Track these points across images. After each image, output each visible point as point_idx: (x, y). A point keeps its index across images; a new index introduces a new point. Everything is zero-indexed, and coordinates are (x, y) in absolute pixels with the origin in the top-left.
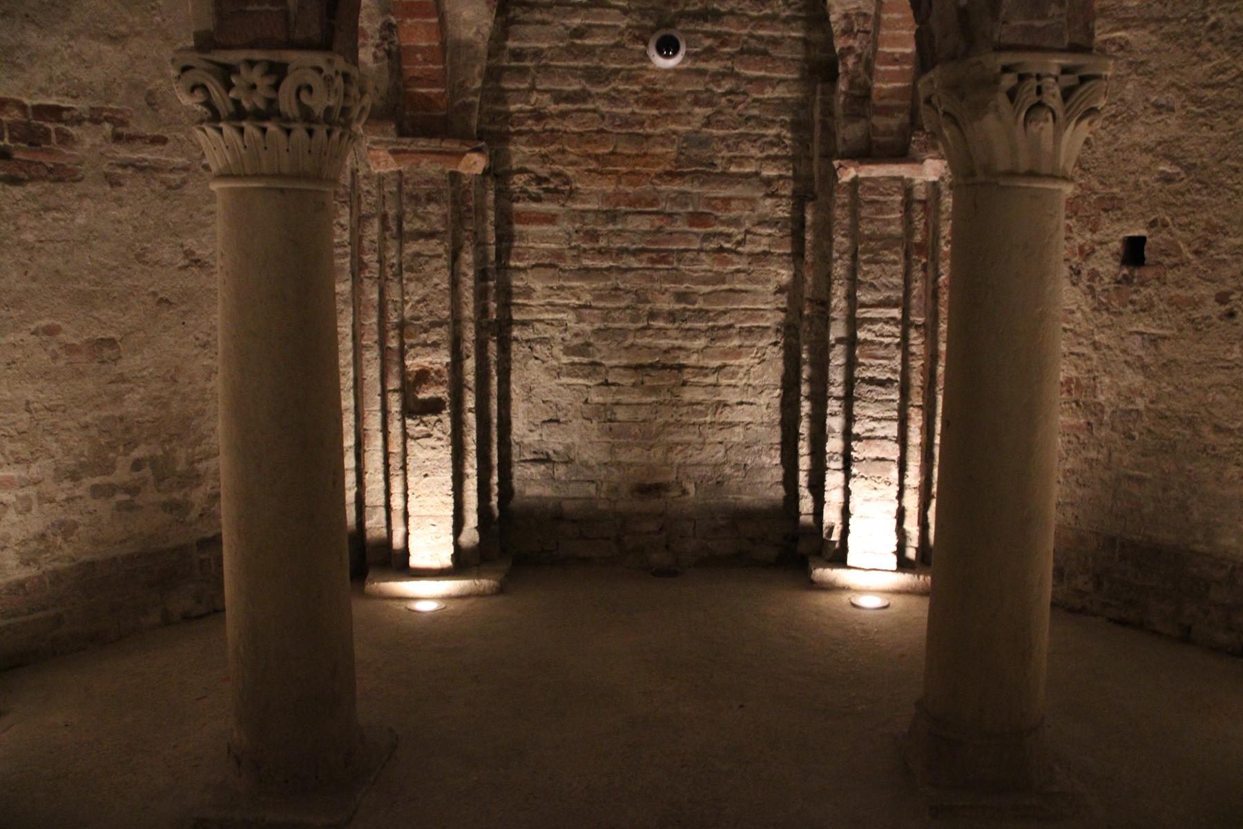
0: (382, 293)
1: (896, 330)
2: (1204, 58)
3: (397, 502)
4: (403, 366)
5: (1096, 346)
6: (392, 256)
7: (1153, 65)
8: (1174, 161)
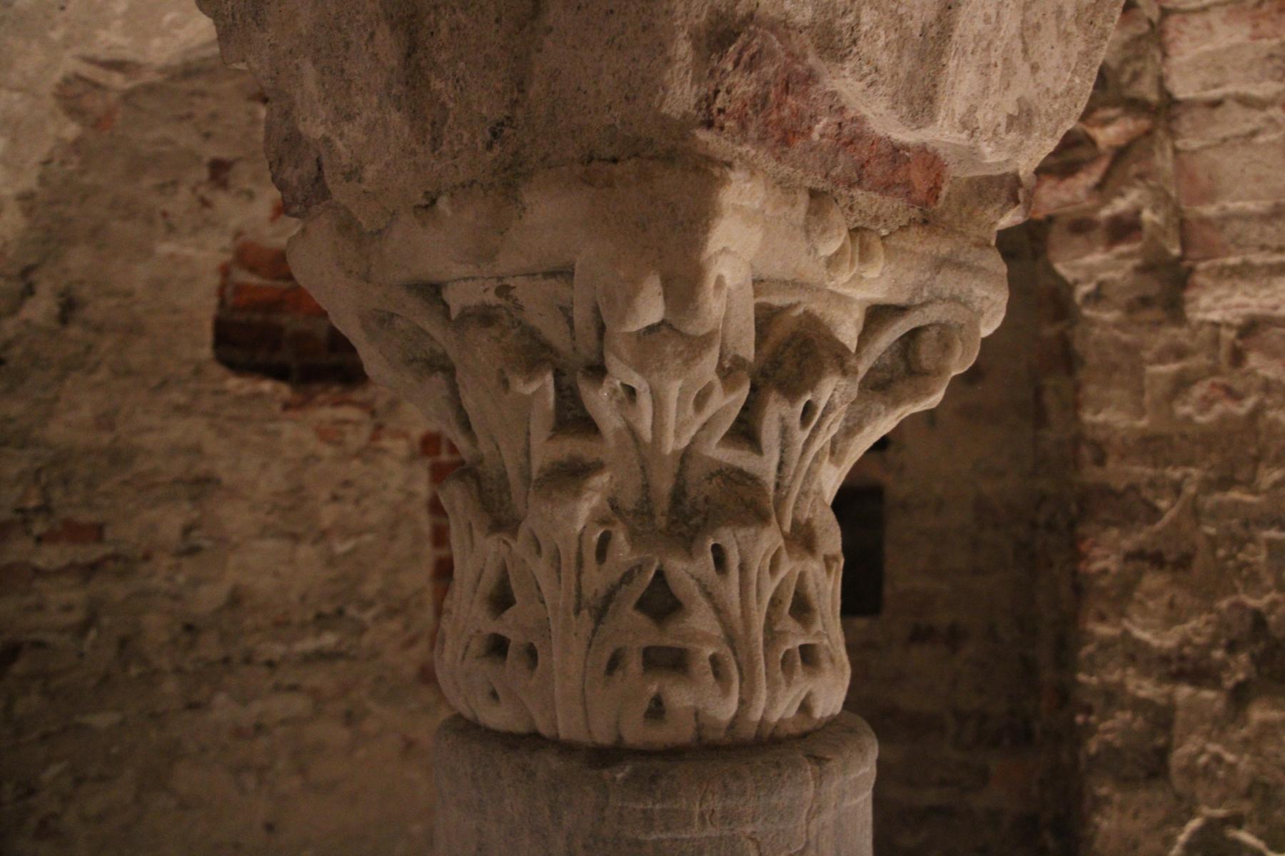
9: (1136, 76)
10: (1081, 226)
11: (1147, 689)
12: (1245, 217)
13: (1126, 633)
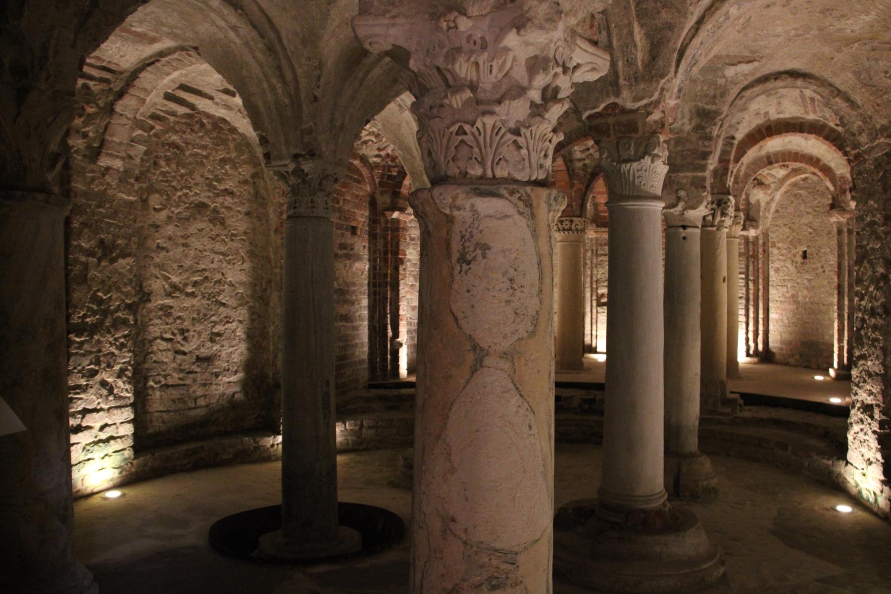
0: (591, 272)
1: (743, 281)
2: (816, 199)
3: (594, 333)
4: (597, 293)
5: (798, 283)
6: (594, 261)
8: (811, 227)
9: (100, 99)
10: (78, 132)
11: (83, 259)
12: (116, 143)
13: (80, 244)
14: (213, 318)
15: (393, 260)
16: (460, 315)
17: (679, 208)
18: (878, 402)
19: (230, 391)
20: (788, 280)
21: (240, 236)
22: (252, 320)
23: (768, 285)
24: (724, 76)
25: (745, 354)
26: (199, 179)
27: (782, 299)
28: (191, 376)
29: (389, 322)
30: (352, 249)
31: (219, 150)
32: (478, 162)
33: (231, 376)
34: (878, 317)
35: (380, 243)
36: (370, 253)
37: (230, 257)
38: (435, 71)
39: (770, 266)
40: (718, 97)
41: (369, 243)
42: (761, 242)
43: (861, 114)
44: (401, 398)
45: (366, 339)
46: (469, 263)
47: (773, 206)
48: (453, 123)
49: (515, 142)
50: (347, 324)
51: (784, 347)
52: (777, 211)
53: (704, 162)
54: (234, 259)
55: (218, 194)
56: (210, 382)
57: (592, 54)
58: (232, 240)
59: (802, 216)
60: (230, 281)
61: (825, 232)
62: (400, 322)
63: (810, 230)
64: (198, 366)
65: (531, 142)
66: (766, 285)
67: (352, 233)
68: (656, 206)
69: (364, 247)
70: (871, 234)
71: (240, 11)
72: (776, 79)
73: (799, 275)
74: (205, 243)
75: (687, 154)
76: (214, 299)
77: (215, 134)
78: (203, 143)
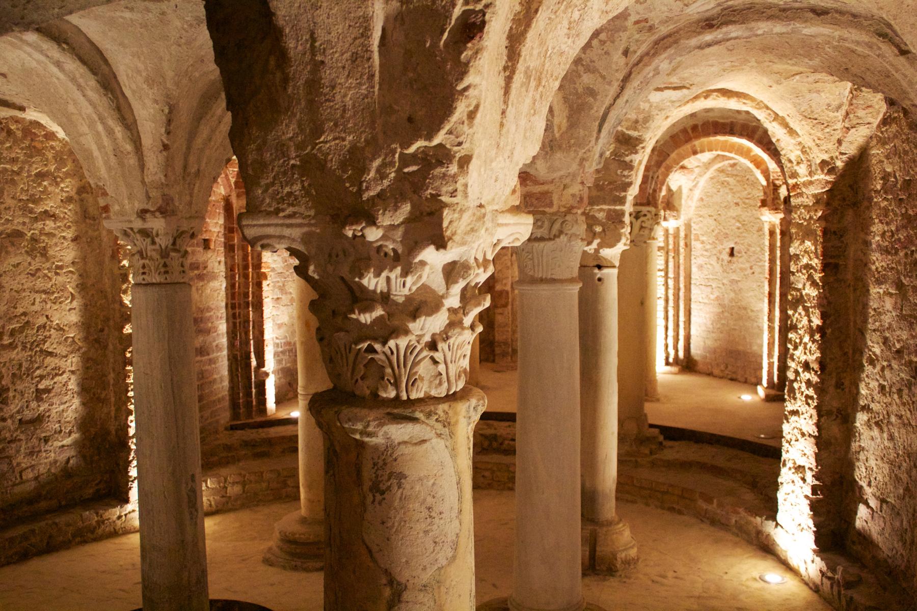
5: (723, 284)
7: (735, 190)
14: (38, 372)
15: (255, 275)
16: (375, 549)
17: (594, 245)
18: (811, 466)
19: (62, 457)
20: (713, 279)
21: (67, 267)
22: (87, 368)
23: (690, 283)
24: (648, 101)
25: (664, 362)
26: (9, 202)
27: (706, 301)
28: (13, 445)
29: (252, 350)
30: (205, 267)
31: (33, 162)
32: (391, 383)
33: (63, 438)
34: (813, 373)
35: (238, 257)
36: (226, 269)
37: (56, 295)
38: (338, 280)
39: (692, 262)
40: (640, 123)
41: (226, 258)
42: (682, 234)
43: (800, 143)
44: (270, 442)
45: (225, 373)
46: (383, 493)
47: (697, 194)
48: (363, 340)
49: (432, 358)
50: (204, 358)
51: (708, 355)
52: (702, 199)
53: (623, 194)
54: (60, 297)
55: (36, 217)
56: (37, 449)
57: (514, 224)
58: (57, 274)
59: (730, 207)
60: (57, 324)
61: (756, 228)
62: (266, 348)
63: (738, 224)
64: (22, 432)
65: (449, 355)
66: (688, 283)
67: (205, 248)
68: (573, 289)
69: (220, 262)
70: (808, 279)
71: (65, 46)
72: (706, 97)
73: (725, 274)
74: (24, 281)
75: (603, 184)
76: (38, 349)
77: (27, 143)
78: (13, 155)
